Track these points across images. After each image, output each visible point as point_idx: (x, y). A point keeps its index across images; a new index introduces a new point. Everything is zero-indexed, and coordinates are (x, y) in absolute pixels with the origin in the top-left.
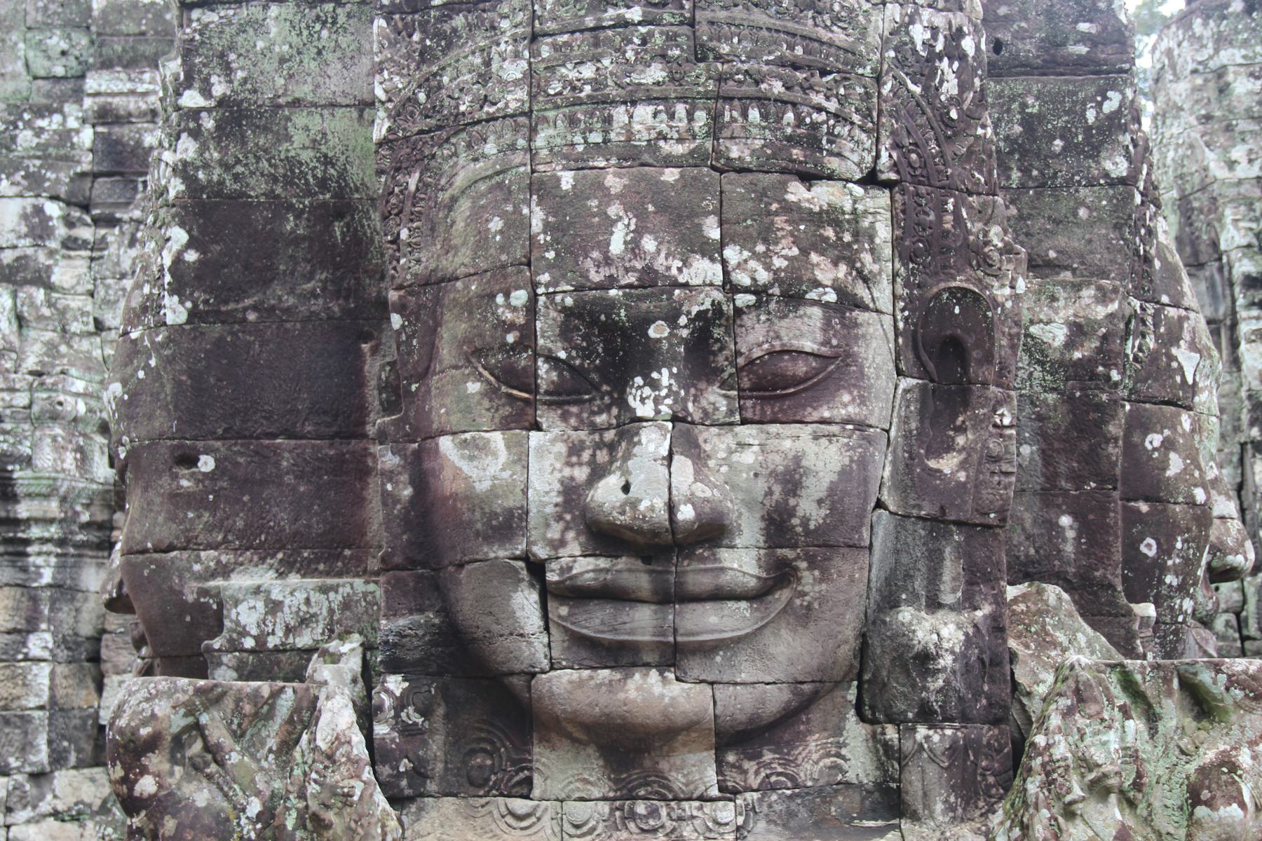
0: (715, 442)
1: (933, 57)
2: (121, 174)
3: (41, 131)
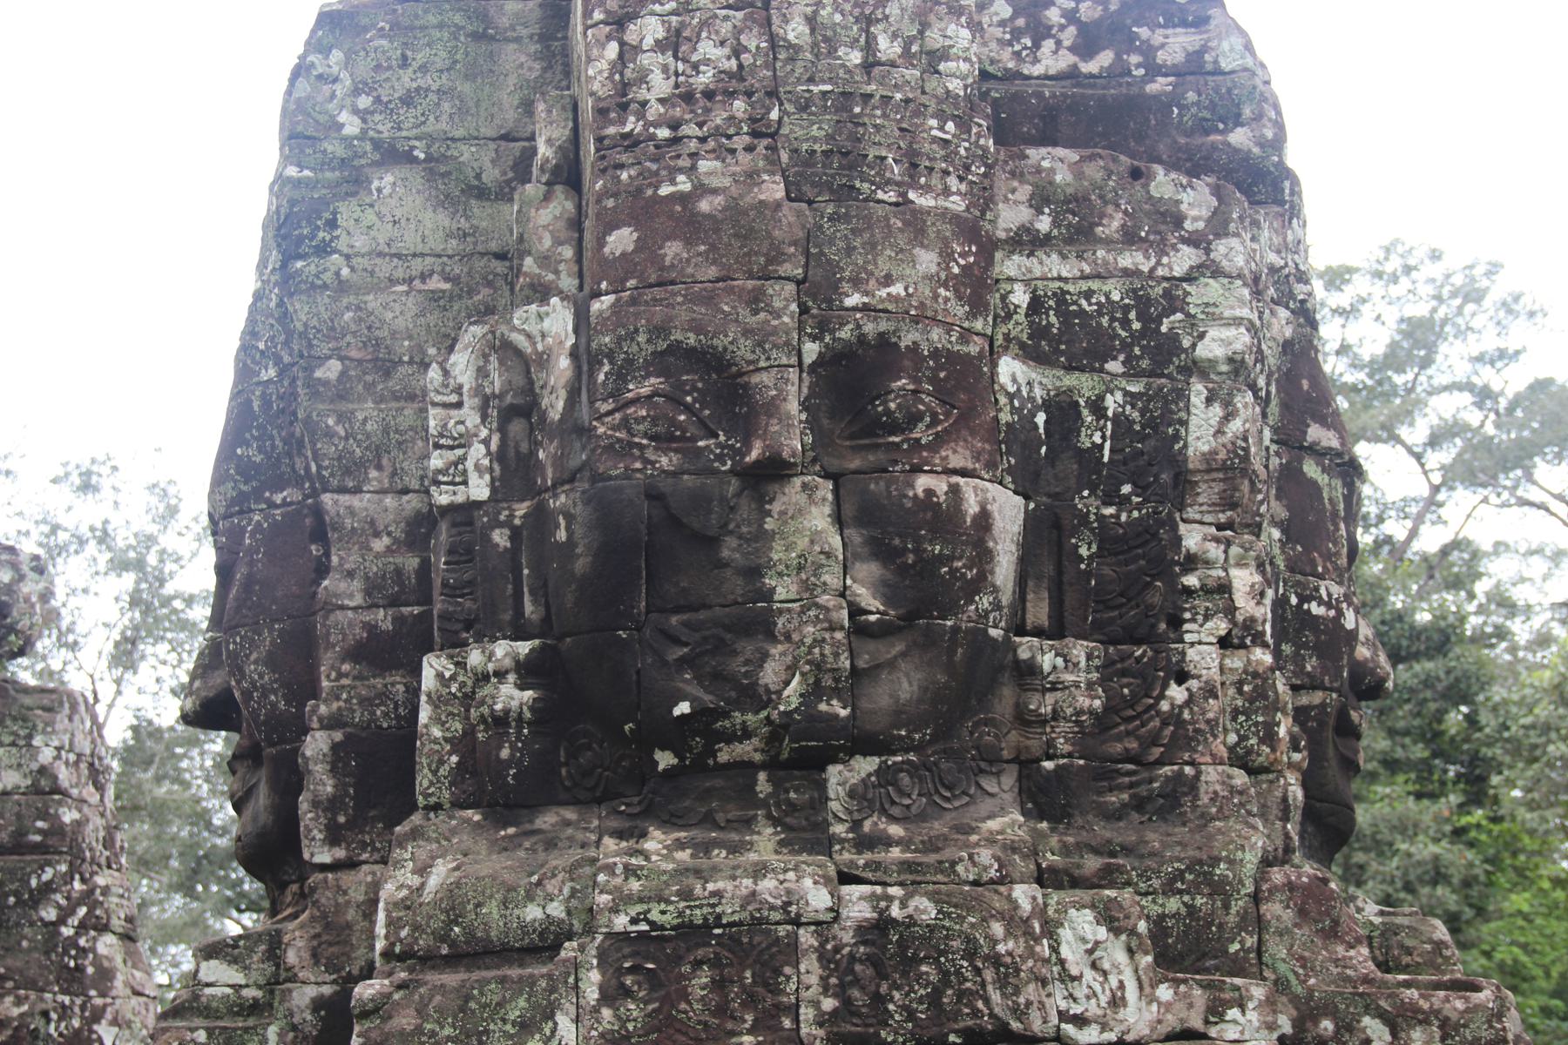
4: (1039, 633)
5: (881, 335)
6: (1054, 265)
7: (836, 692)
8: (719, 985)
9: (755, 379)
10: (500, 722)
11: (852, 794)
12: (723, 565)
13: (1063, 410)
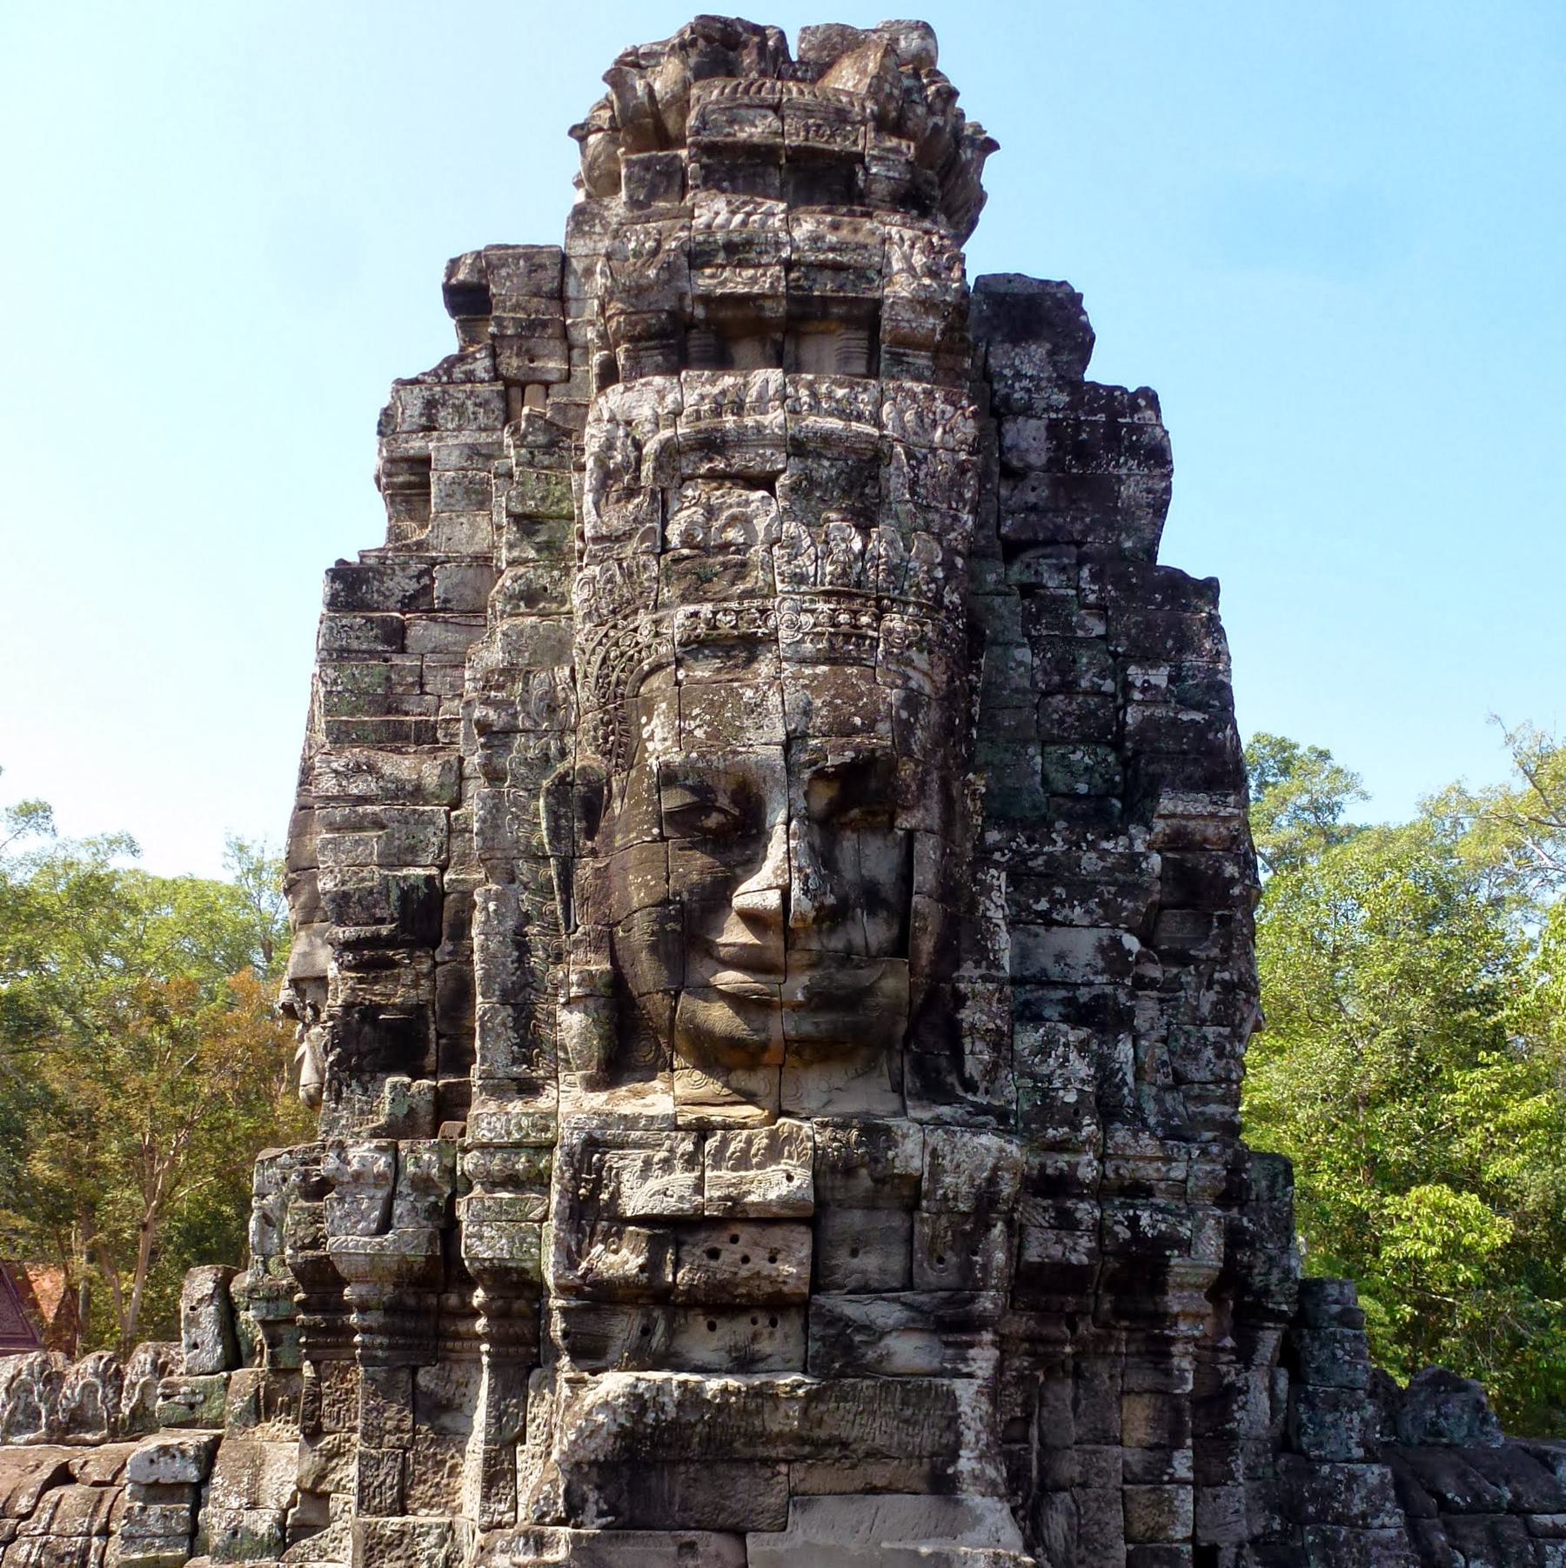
2: (1194, 907)
3: (1104, 854)
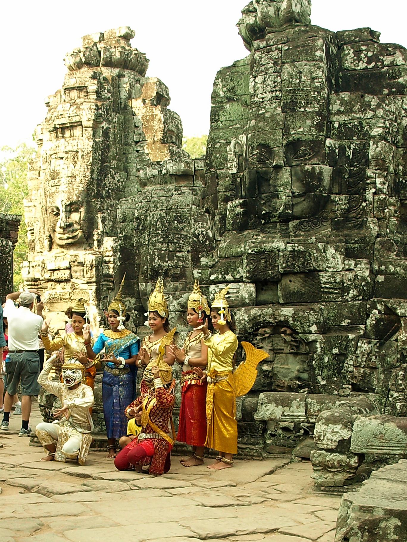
0: (168, 284)
1: (199, 235)
4: (337, 194)
5: (298, 139)
6: (343, 118)
7: (289, 209)
8: (265, 262)
9: (274, 149)
10: (237, 215)
11: (294, 227)
12: (270, 185)
13: (342, 149)
